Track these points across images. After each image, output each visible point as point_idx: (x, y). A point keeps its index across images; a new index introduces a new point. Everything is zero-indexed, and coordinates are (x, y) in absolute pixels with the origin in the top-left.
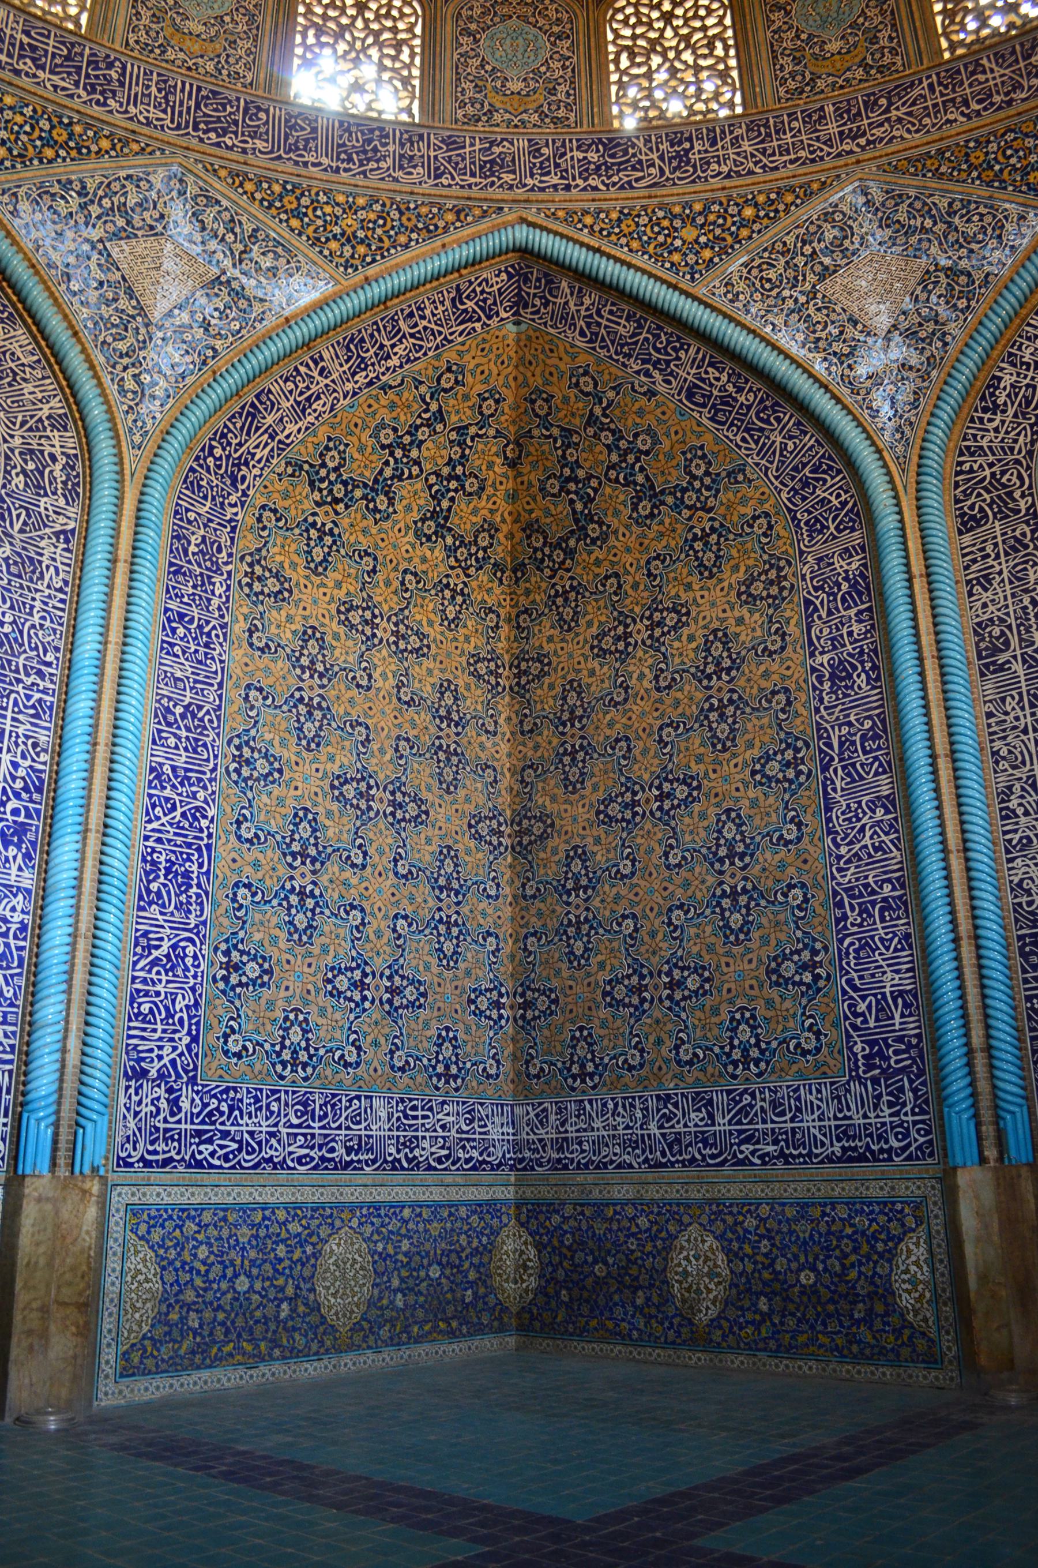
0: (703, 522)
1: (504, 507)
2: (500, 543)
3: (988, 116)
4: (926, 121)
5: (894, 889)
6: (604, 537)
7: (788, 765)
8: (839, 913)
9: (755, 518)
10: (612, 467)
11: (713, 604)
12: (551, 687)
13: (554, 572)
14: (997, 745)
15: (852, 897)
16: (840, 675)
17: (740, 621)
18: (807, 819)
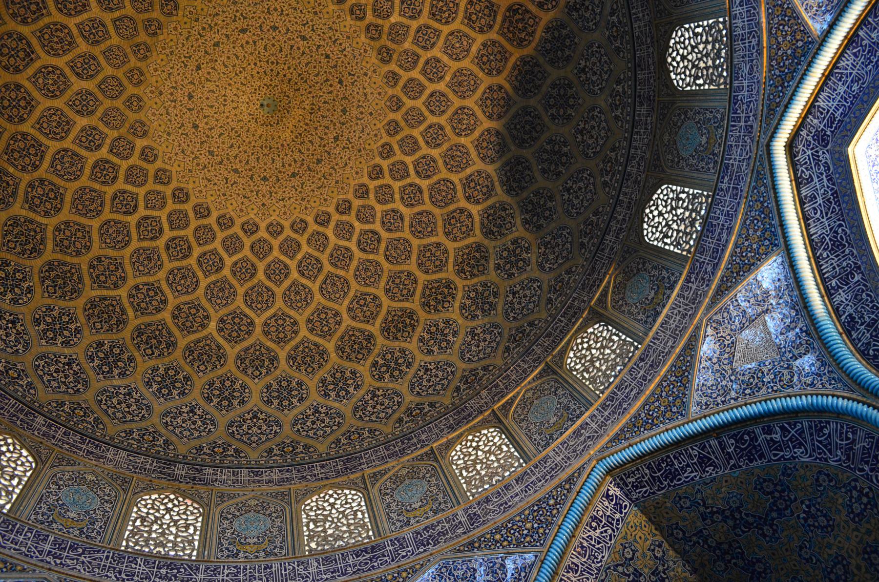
4: (96, 570)
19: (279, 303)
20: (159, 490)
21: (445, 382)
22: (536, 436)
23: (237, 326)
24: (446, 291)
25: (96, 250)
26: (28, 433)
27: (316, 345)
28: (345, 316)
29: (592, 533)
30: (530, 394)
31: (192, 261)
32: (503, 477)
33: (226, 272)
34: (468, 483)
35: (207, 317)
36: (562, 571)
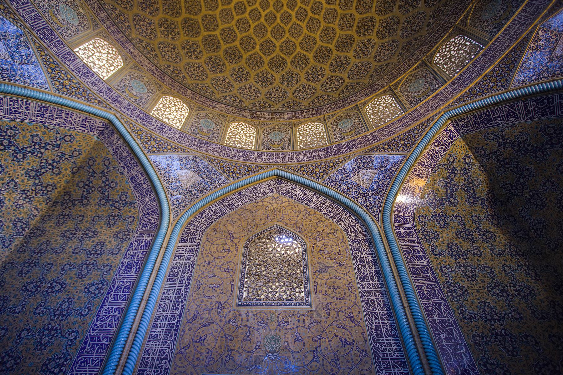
0: (116, 212)
1: (63, 184)
2: (54, 193)
3: (227, 158)
5: (107, 341)
6: (87, 205)
7: (98, 289)
8: (84, 345)
9: (131, 217)
10: (101, 187)
11: (105, 235)
12: (40, 240)
13: (66, 208)
14: (162, 303)
15: (91, 341)
16: (129, 267)
17: (110, 242)
18: (93, 309)
19: (287, 35)
20: (238, 121)
21: (366, 72)
22: (412, 99)
23: (268, 47)
24: (370, 23)
25: (204, 12)
26: (185, 97)
27: (304, 55)
28: (318, 40)
29: (434, 148)
30: (410, 78)
31: (247, 15)
32: (391, 119)
33: (262, 20)
34: (374, 120)
35: (255, 43)
36: (416, 165)
